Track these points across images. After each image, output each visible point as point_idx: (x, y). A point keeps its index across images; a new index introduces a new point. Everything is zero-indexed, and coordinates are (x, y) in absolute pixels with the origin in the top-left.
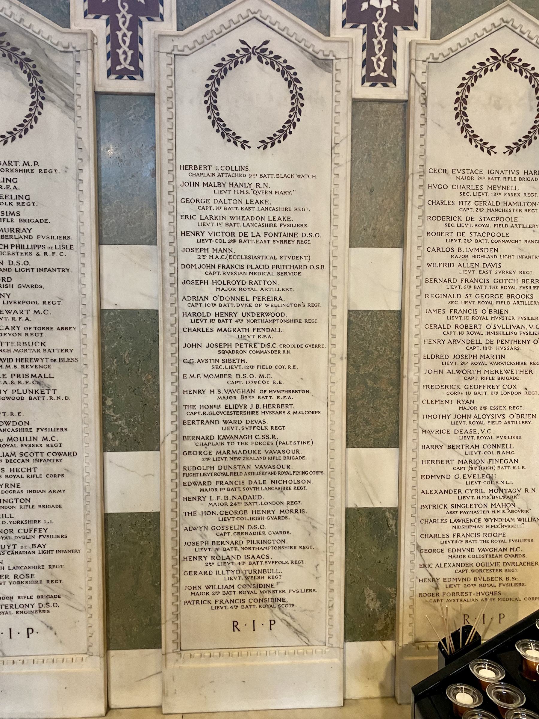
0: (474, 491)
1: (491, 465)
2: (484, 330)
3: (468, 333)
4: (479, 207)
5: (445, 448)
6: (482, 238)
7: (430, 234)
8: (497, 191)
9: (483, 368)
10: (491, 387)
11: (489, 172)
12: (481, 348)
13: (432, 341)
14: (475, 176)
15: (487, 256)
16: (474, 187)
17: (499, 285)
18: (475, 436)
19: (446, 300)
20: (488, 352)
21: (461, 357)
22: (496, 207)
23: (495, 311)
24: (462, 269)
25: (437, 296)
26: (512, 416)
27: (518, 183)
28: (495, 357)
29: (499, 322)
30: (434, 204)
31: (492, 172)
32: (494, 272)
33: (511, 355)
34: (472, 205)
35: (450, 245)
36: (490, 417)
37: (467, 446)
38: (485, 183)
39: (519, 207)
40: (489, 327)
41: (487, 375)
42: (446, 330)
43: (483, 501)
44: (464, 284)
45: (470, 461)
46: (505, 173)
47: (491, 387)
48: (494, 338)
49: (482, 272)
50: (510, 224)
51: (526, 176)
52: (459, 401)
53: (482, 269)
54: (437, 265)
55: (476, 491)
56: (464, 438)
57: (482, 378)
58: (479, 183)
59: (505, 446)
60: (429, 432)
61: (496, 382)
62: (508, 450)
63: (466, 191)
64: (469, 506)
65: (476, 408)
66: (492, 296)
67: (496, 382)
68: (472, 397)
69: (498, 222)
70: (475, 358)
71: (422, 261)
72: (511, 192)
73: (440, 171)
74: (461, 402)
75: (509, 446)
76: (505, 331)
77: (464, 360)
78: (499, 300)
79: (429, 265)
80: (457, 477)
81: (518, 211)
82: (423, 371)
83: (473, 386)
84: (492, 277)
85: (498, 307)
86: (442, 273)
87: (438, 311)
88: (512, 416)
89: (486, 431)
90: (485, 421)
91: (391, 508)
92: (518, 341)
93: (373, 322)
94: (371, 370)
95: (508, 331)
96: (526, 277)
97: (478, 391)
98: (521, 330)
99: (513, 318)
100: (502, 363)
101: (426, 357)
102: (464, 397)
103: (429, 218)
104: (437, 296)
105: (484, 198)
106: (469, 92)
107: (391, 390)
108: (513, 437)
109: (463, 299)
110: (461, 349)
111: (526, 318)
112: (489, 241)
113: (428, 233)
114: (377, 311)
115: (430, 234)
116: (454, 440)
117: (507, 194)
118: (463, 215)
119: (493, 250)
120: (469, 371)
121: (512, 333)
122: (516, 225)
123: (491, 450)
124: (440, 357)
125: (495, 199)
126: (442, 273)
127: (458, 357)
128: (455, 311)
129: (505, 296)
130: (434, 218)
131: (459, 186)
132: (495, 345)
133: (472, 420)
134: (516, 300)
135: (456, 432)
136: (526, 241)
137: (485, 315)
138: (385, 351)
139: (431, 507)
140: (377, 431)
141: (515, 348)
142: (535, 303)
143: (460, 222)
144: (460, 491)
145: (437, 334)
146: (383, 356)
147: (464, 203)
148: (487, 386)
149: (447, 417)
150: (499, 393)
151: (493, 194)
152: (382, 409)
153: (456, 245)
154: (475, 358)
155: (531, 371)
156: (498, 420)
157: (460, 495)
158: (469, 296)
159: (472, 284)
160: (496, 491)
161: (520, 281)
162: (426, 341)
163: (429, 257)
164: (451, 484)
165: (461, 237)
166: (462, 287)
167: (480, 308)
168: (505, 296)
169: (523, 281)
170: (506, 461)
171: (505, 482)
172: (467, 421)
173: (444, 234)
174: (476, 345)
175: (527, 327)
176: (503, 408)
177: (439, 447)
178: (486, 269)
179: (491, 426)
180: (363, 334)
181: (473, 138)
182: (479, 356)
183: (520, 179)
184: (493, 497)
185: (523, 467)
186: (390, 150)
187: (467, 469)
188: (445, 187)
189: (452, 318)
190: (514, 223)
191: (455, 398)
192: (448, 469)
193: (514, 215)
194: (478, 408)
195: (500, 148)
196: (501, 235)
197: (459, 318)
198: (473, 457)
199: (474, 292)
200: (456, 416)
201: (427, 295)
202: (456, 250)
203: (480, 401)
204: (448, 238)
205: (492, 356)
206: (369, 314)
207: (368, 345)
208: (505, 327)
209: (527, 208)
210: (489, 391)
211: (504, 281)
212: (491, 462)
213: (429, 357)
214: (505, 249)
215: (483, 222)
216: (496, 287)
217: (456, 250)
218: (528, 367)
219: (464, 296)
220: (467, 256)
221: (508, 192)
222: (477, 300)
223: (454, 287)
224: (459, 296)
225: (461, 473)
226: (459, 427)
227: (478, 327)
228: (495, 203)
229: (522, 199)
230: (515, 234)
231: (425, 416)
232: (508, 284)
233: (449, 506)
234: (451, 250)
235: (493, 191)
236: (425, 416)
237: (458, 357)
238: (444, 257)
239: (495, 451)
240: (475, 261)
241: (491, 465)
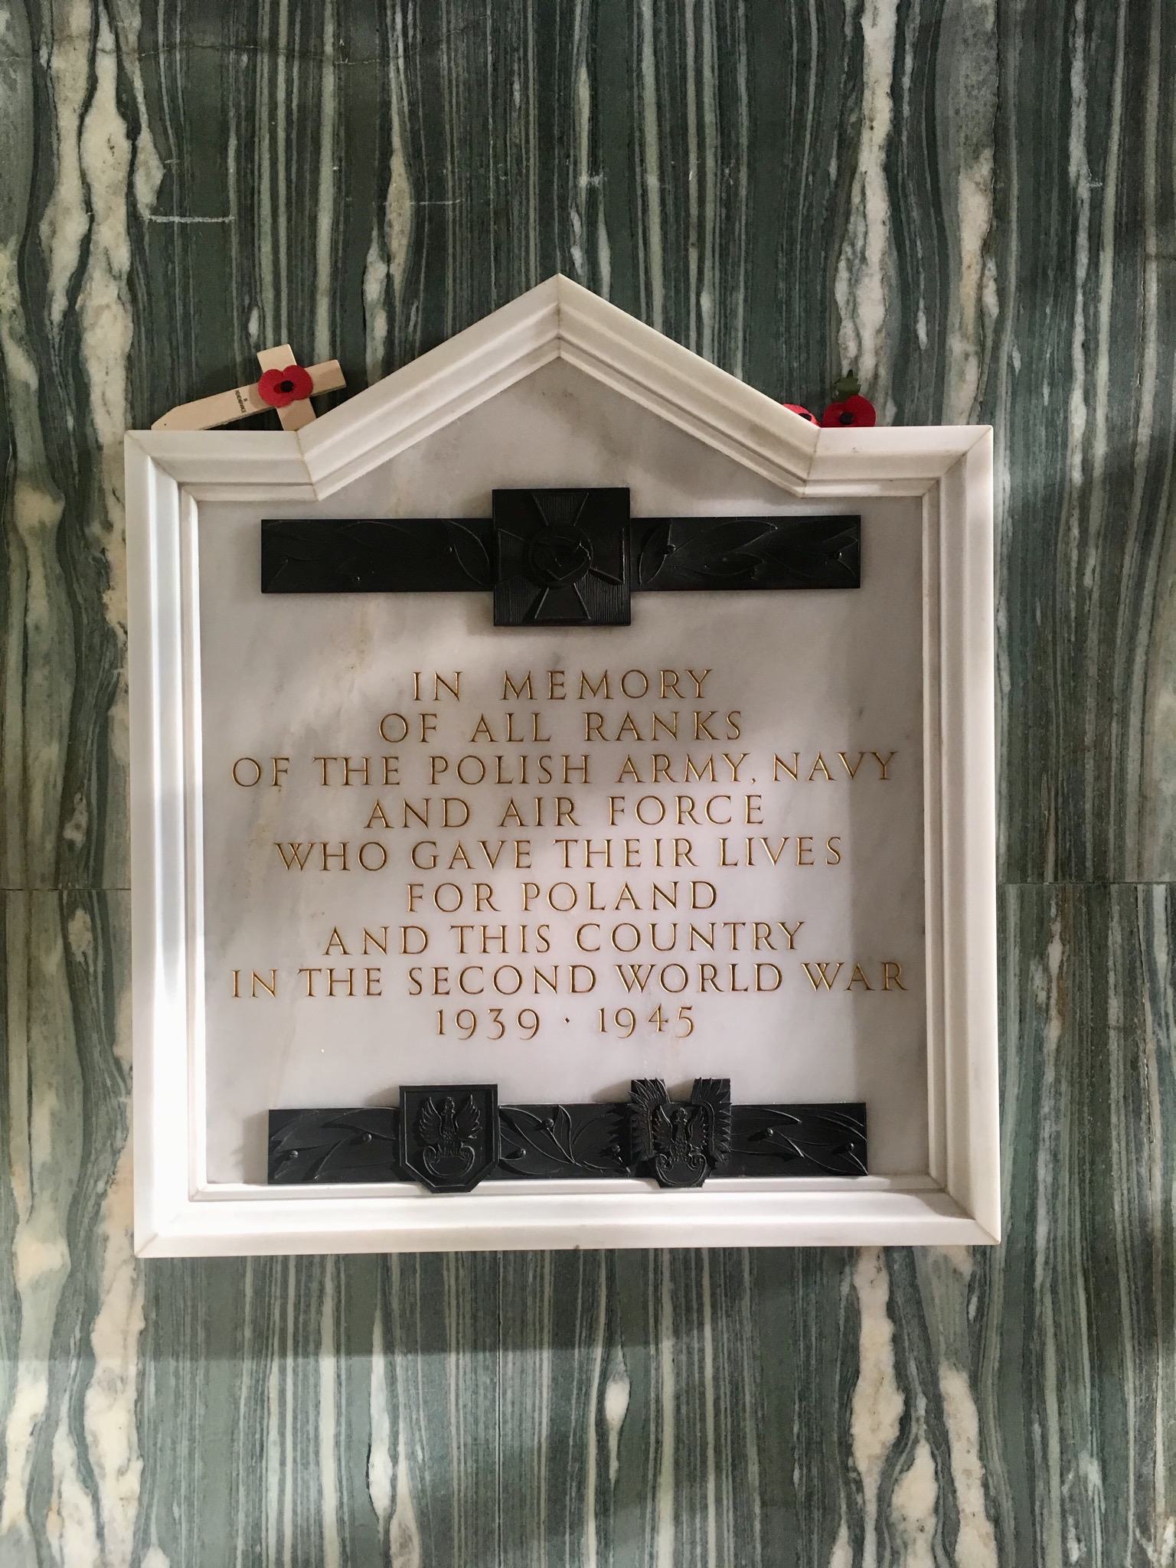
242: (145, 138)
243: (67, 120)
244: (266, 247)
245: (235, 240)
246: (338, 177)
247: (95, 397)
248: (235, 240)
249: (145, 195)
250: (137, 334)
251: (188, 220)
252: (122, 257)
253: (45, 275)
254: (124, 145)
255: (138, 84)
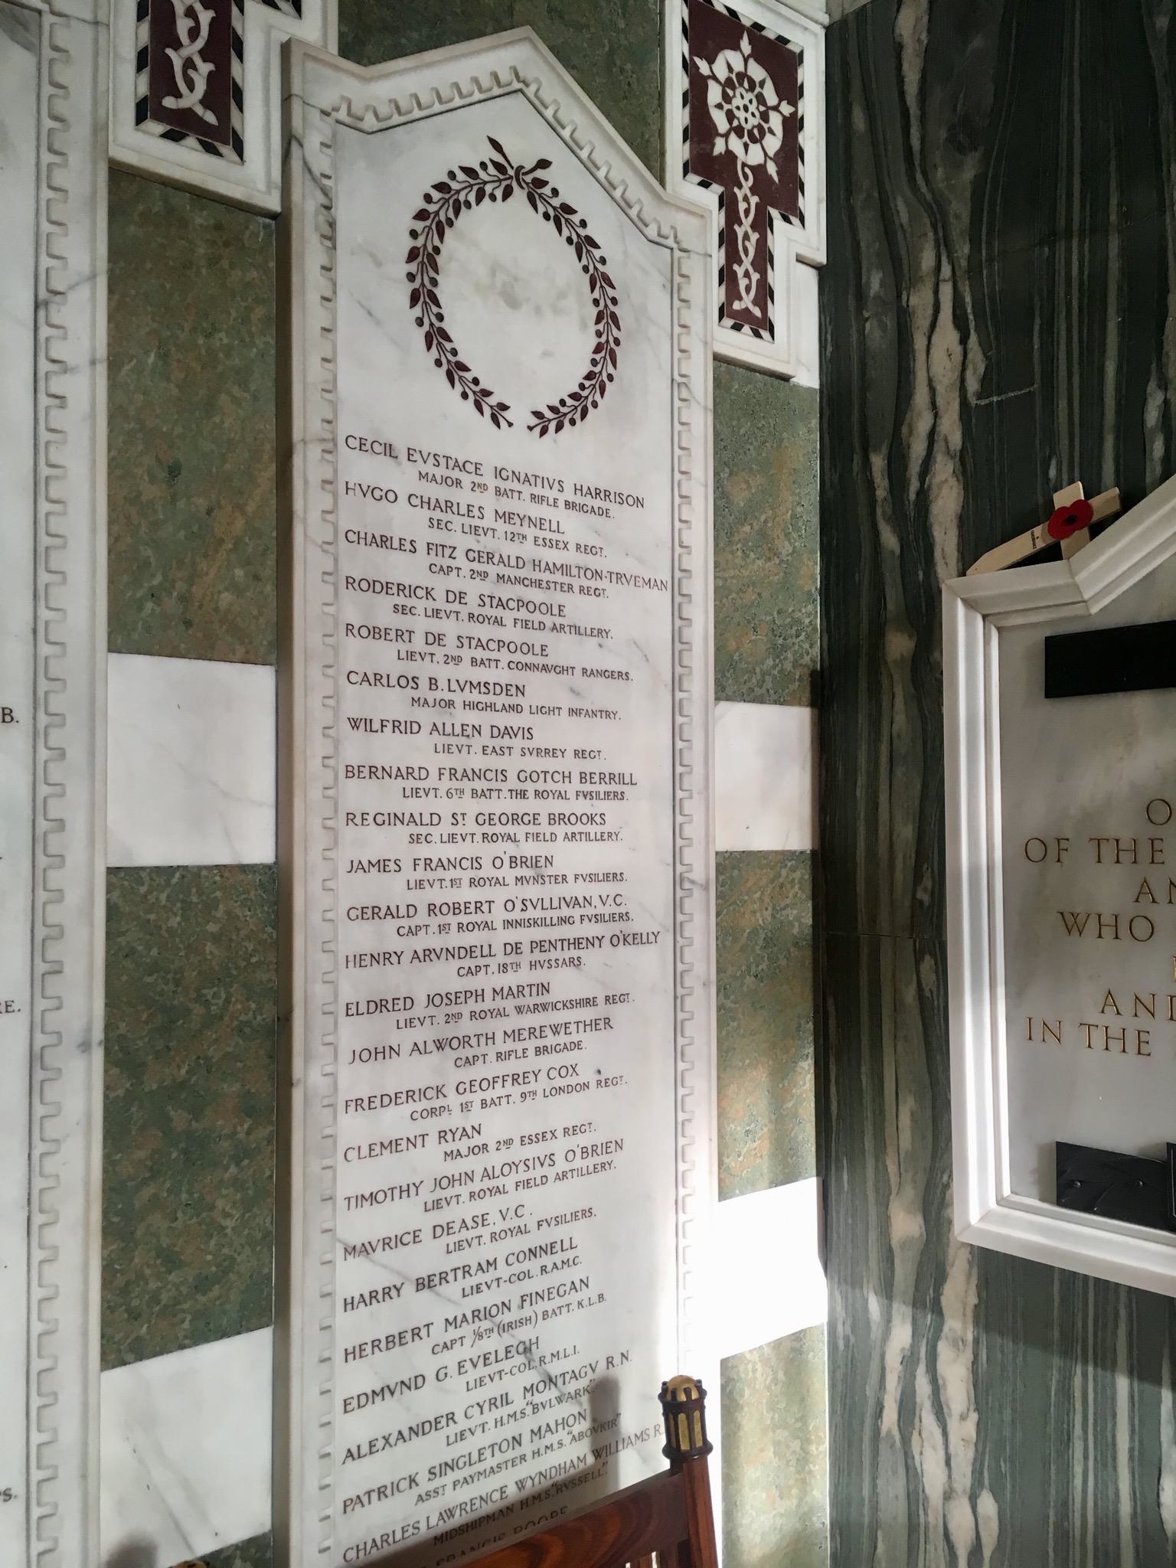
0: (486, 1407)
1: (528, 1311)
2: (499, 915)
3: (460, 926)
4: (476, 566)
5: (408, 1290)
6: (486, 655)
7: (355, 631)
8: (517, 529)
9: (498, 1026)
10: (521, 1080)
11: (498, 473)
12: (494, 968)
13: (368, 958)
14: (467, 479)
15: (499, 707)
16: (463, 510)
17: (530, 787)
18: (485, 1232)
19: (403, 832)
20: (510, 980)
21: (445, 1000)
22: (517, 570)
23: (523, 861)
24: (441, 740)
25: (379, 819)
26: (570, 1156)
27: (559, 515)
28: (527, 991)
29: (532, 892)
30: (362, 541)
31: (504, 474)
32: (516, 752)
33: (565, 983)
34: (461, 560)
35: (411, 668)
36: (522, 1167)
37: (466, 1270)
38: (489, 502)
39: (566, 580)
40: (510, 905)
41: (510, 1045)
42: (405, 922)
43: (509, 1430)
44: (446, 784)
45: (476, 1314)
46: (533, 482)
47: (521, 1080)
48: (524, 935)
49: (489, 750)
50: (549, 621)
51: (579, 499)
52: (442, 1135)
53: (491, 743)
54: (376, 726)
55: (493, 1403)
56: (459, 1246)
57: (499, 1056)
58: (477, 498)
59: (558, 1247)
60: (365, 1250)
61: (532, 1062)
62: (565, 1256)
63: (444, 517)
64: (475, 1457)
65: (485, 1147)
66: (515, 819)
67: (532, 1062)
68: (476, 1116)
69: (523, 614)
70: (480, 998)
71: (336, 716)
72: (548, 535)
73: (377, 448)
74: (449, 1137)
75: (566, 1245)
76: (548, 914)
77: (453, 1009)
78: (532, 829)
79: (355, 724)
80: (441, 1376)
81: (566, 588)
82: (345, 1056)
83: (477, 1084)
84: (512, 764)
85: (529, 849)
86: (390, 749)
87: (382, 865)
88: (570, 1156)
89: (512, 1213)
90: (509, 1182)
91: (252, 1541)
92: (577, 943)
93: (187, 906)
94: (183, 1071)
95: (555, 914)
96: (589, 766)
97: (489, 1095)
98: (582, 911)
99: (564, 878)
100: (545, 1007)
101: (353, 1011)
102: (454, 1120)
103: (350, 581)
104: (379, 819)
105: (486, 543)
106: (442, 242)
107: (248, 1133)
108: (575, 1216)
109: (446, 828)
110: (444, 976)
111: (592, 878)
112: (503, 664)
113: (349, 627)
114: (200, 868)
115: (355, 631)
116: (428, 1258)
117: (540, 542)
118: (441, 584)
119: (513, 690)
120: (465, 1041)
121: (563, 921)
122: (562, 627)
123: (526, 1266)
124: (390, 1006)
125: (510, 550)
126: (390, 749)
127: (437, 1000)
128: (428, 862)
129: (543, 819)
130: (364, 585)
131: (425, 499)
132: (526, 957)
133: (476, 1186)
134: (570, 829)
135: (439, 1231)
136: (584, 671)
137: (499, 874)
138: (227, 1001)
139: (374, 1496)
140: (202, 1284)
141: (571, 960)
142: (610, 835)
143: (430, 604)
144: (451, 1417)
145: (383, 936)
146: (221, 1018)
147: (440, 549)
148: (510, 1079)
149: (413, 1189)
150: (540, 1093)
151: (510, 536)
152: (220, 1203)
153: (423, 670)
154: (480, 998)
155: (607, 1021)
156: (539, 1172)
157: (452, 1430)
158: (459, 818)
159: (467, 785)
160: (541, 1387)
161: (576, 778)
162: (351, 959)
163: (357, 701)
164: (426, 1403)
165: (434, 648)
166: (442, 792)
167: (487, 852)
168: (543, 819)
169: (583, 777)
170: (561, 1292)
171: (562, 1355)
172: (464, 1191)
173: (393, 635)
174: (481, 962)
175: (596, 901)
176: (549, 1136)
177: (394, 1293)
178: (498, 742)
179: (525, 1196)
180: (154, 952)
181: (455, 371)
182: (489, 994)
183: (567, 504)
184: (535, 1408)
185: (601, 1297)
186: (228, 355)
187: (467, 1342)
188: (391, 496)
189: (420, 884)
190: (559, 621)
191: (433, 1125)
192: (419, 1358)
193: (557, 598)
194: (492, 1147)
195: (520, 415)
196: (531, 648)
197: (437, 884)
198: (486, 1300)
199: (471, 806)
200: (438, 1183)
201: (350, 817)
202: (424, 683)
203: (496, 1124)
204: (404, 647)
205: (520, 989)
206: (174, 880)
207: (171, 987)
208: (547, 904)
209: (586, 583)
210: (516, 1091)
211: (542, 776)
212: (527, 1304)
213: (363, 1008)
214: (540, 688)
215: (487, 611)
216: (523, 794)
217: (424, 683)
218: (600, 1011)
219: (447, 819)
220: (450, 704)
221: (541, 534)
222: (479, 831)
223: (421, 793)
224: (435, 818)
225: (450, 1359)
226: (441, 1217)
227: (485, 908)
228: (513, 562)
229: (570, 557)
230: (564, 649)
231: (353, 1201)
232: (550, 786)
233: (422, 1477)
234: (412, 684)
235: (509, 528)
236: (353, 1201)
237: (437, 1000)
238: (392, 704)
239: (534, 1265)
240: (472, 717)
241: (528, 1311)
242: (973, 338)
243: (920, 343)
244: (1063, 404)
245: (1038, 403)
246: (1121, 327)
247: (938, 554)
248: (1038, 403)
249: (973, 385)
250: (966, 497)
251: (1003, 397)
252: (956, 440)
253: (905, 468)
254: (958, 350)
255: (968, 299)
